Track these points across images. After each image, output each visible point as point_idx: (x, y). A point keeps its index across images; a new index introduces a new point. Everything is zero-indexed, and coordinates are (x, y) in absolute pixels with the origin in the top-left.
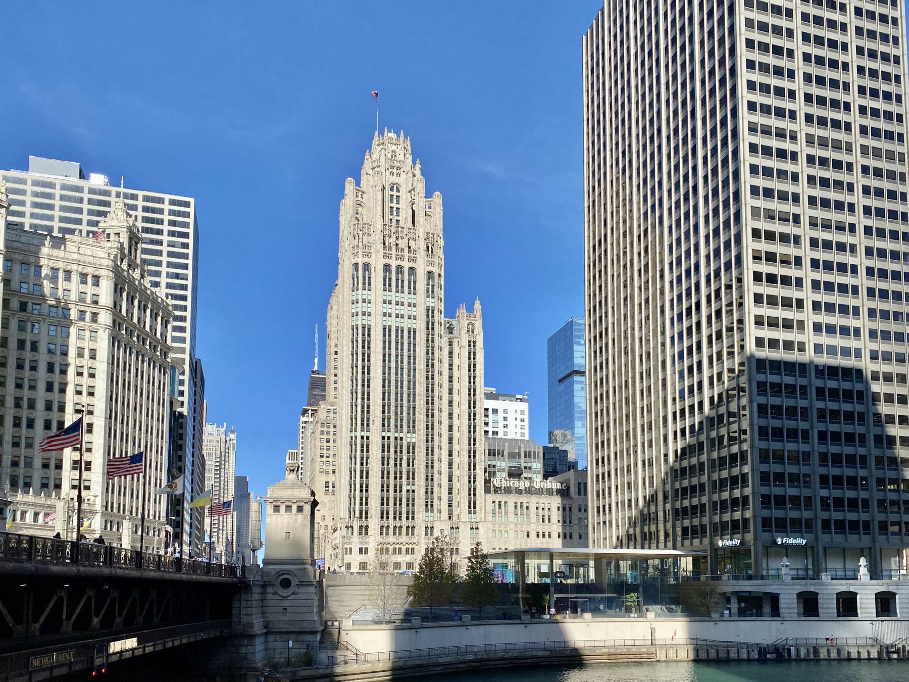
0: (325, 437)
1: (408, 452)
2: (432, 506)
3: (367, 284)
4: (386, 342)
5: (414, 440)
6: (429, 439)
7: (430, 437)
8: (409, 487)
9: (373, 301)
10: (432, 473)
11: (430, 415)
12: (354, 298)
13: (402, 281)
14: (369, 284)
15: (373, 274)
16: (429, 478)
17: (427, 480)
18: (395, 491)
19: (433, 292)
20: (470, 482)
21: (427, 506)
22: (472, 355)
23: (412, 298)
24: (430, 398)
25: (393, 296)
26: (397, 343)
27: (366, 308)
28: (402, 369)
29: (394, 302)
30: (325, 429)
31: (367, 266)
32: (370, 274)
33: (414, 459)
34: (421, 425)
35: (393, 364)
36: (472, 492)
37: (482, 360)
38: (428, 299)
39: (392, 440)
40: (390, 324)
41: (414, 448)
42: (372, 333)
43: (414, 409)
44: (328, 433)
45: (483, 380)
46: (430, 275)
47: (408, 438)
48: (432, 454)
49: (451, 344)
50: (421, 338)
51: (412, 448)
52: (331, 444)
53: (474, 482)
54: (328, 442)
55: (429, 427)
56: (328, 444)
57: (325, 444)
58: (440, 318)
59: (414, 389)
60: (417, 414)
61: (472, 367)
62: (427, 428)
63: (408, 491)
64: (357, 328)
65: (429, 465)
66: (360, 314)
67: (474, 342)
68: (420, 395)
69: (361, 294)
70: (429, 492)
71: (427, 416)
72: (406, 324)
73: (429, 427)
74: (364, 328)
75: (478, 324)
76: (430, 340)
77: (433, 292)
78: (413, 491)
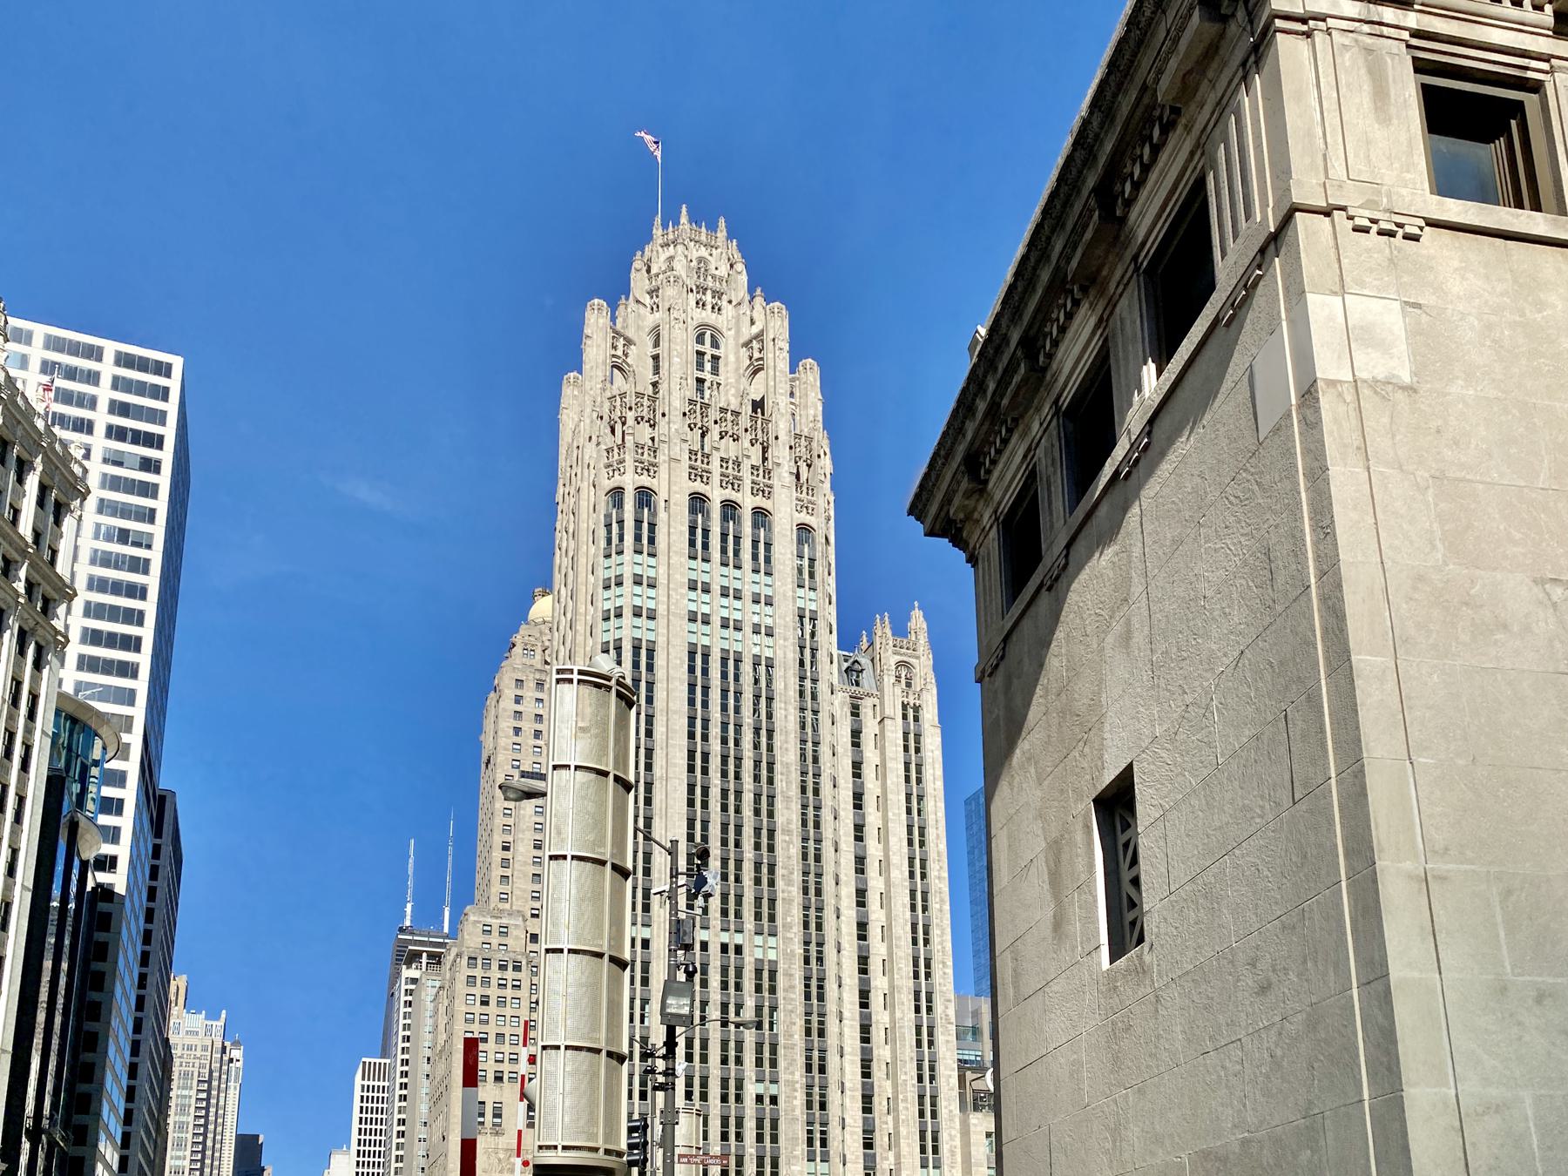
0: (478, 991)
1: (758, 989)
2: (824, 1143)
3: (647, 539)
4: (696, 691)
5: (772, 955)
6: (814, 954)
7: (813, 948)
8: (760, 1089)
9: (662, 580)
10: (823, 1051)
11: (813, 889)
12: (612, 574)
13: (737, 539)
14: (652, 541)
15: (662, 516)
16: (816, 1066)
17: (809, 1068)
18: (724, 1099)
19: (812, 575)
20: (920, 1079)
21: (810, 1142)
22: (913, 743)
23: (762, 585)
24: (811, 844)
25: (716, 574)
26: (725, 692)
27: (646, 601)
28: (739, 759)
29: (716, 589)
30: (478, 972)
31: (645, 497)
32: (653, 514)
33: (773, 1009)
34: (790, 912)
35: (715, 747)
36: (928, 1106)
37: (938, 754)
38: (801, 592)
39: (714, 949)
40: (706, 641)
41: (773, 975)
42: (660, 660)
43: (772, 868)
44: (486, 981)
45: (942, 805)
46: (804, 530)
47: (756, 949)
48: (821, 998)
49: (855, 712)
50: (786, 683)
51: (767, 977)
52: (492, 1009)
53: (932, 1078)
54: (485, 1003)
55: (813, 923)
56: (485, 1009)
57: (478, 1009)
58: (828, 642)
59: (771, 815)
60: (780, 884)
61: (913, 773)
62: (806, 925)
63: (759, 1099)
64: (618, 649)
65: (815, 1029)
66: (628, 612)
67: (916, 709)
68: (788, 832)
69: (629, 563)
70: (818, 1103)
71: (805, 891)
72: (750, 645)
73: (813, 923)
74: (636, 649)
75: (924, 666)
76: (808, 698)
77: (812, 575)
78: (774, 1100)
